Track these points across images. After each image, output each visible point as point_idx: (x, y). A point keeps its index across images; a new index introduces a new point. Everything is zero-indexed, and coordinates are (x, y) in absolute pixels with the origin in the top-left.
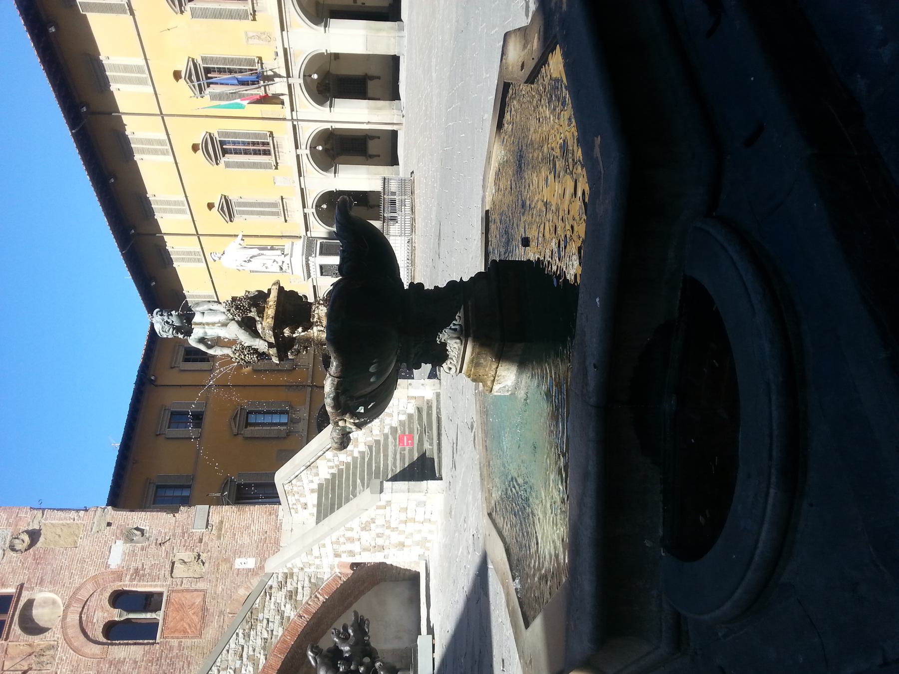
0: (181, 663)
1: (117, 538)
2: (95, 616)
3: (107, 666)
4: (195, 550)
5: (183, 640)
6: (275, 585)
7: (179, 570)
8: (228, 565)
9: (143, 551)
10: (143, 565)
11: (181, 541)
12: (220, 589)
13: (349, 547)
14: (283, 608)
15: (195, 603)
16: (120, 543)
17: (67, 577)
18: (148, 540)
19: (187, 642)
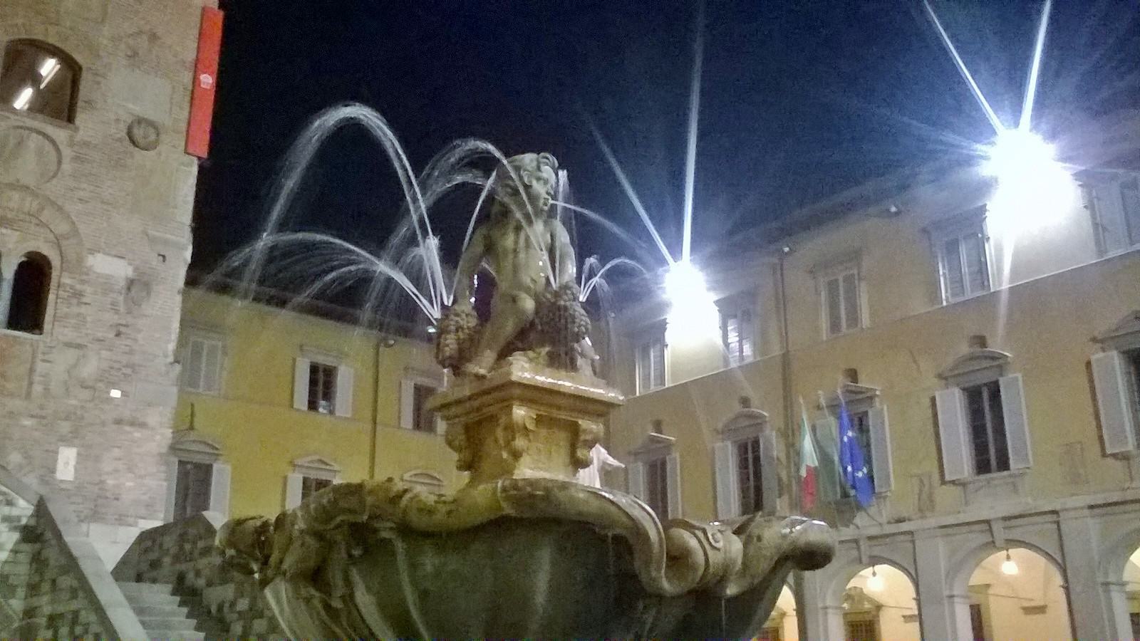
1: (136, 269)
6: (15, 512)
9: (112, 304)
10: (86, 304)
11: (119, 362)
16: (130, 272)
17: (81, 194)
18: (128, 313)
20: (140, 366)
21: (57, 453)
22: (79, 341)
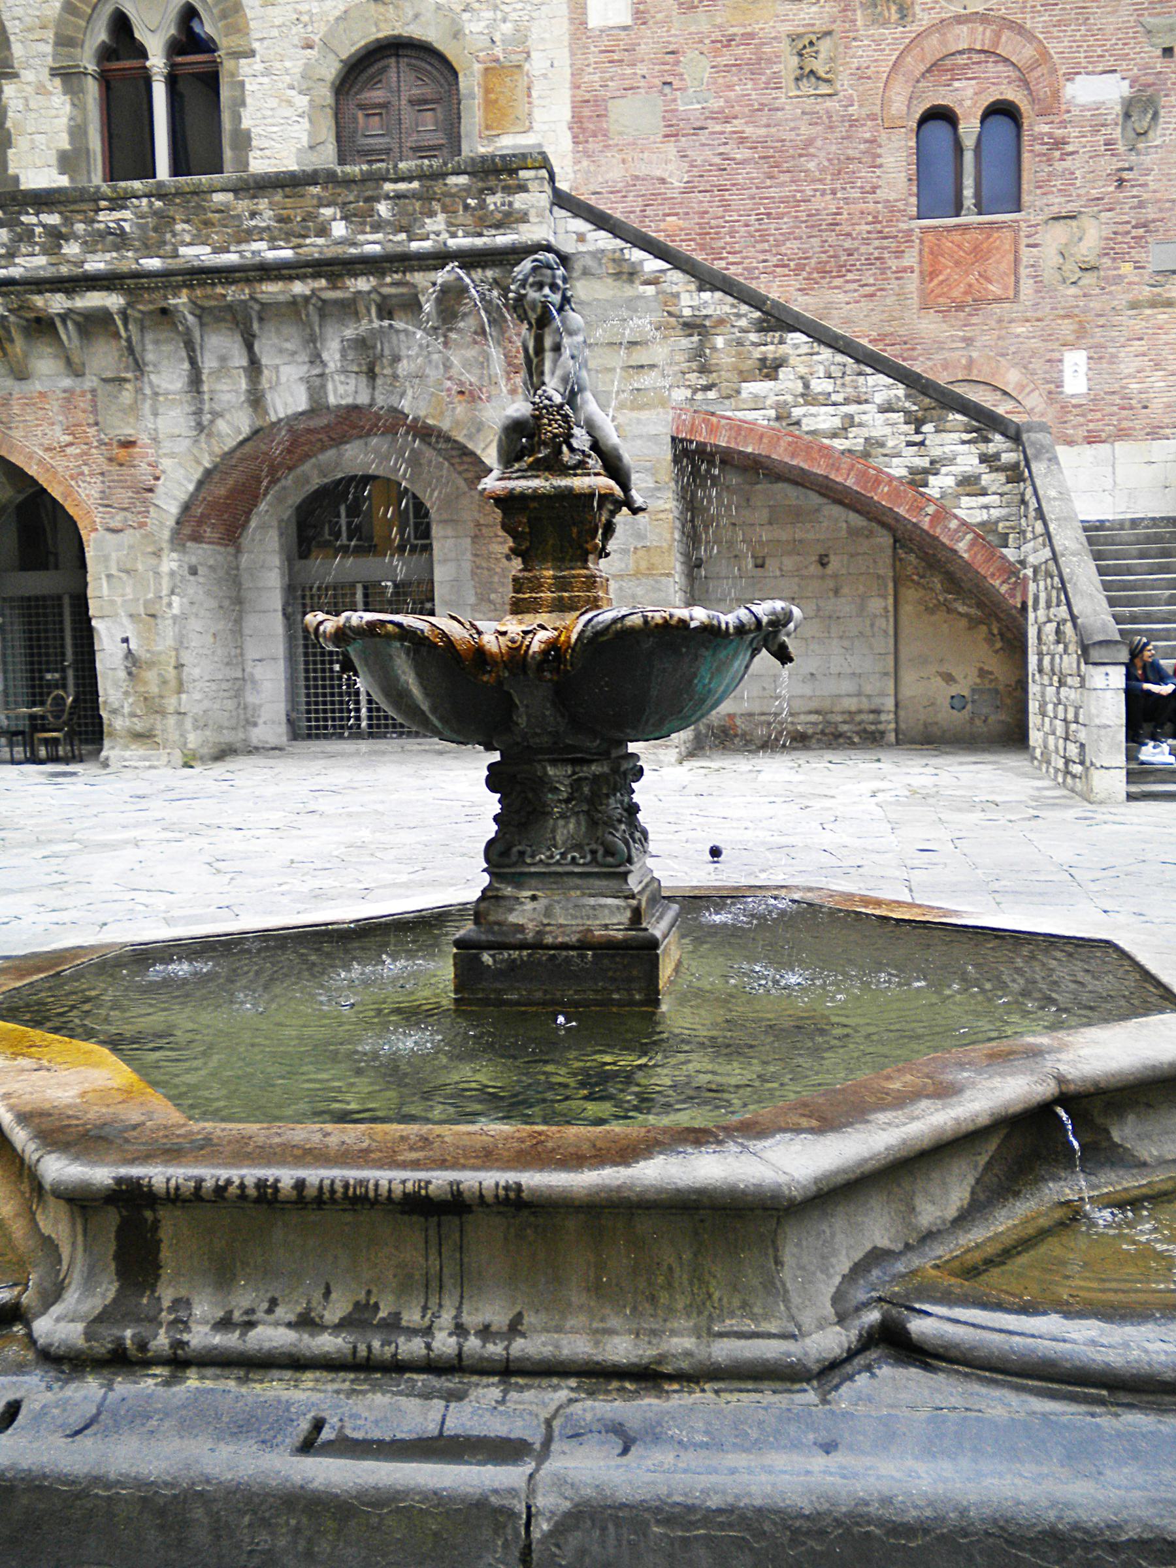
0: (871, 281)
2: (964, 83)
3: (868, 135)
4: (1105, 260)
5: (915, 275)
6: (991, 448)
7: (1058, 234)
8: (1071, 338)
10: (1072, 153)
11: (1128, 222)
12: (1019, 330)
13: (1043, 596)
14: (944, 470)
15: (990, 282)
19: (912, 283)
20: (1154, 221)
21: (1061, 361)
22: (1069, 207)
